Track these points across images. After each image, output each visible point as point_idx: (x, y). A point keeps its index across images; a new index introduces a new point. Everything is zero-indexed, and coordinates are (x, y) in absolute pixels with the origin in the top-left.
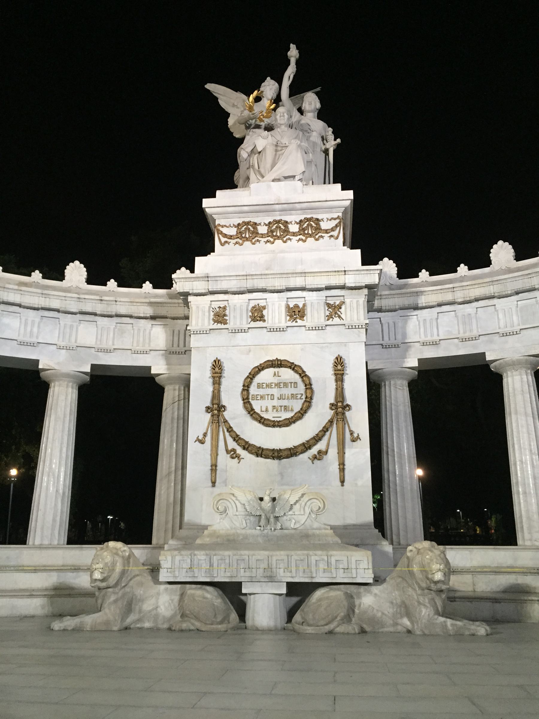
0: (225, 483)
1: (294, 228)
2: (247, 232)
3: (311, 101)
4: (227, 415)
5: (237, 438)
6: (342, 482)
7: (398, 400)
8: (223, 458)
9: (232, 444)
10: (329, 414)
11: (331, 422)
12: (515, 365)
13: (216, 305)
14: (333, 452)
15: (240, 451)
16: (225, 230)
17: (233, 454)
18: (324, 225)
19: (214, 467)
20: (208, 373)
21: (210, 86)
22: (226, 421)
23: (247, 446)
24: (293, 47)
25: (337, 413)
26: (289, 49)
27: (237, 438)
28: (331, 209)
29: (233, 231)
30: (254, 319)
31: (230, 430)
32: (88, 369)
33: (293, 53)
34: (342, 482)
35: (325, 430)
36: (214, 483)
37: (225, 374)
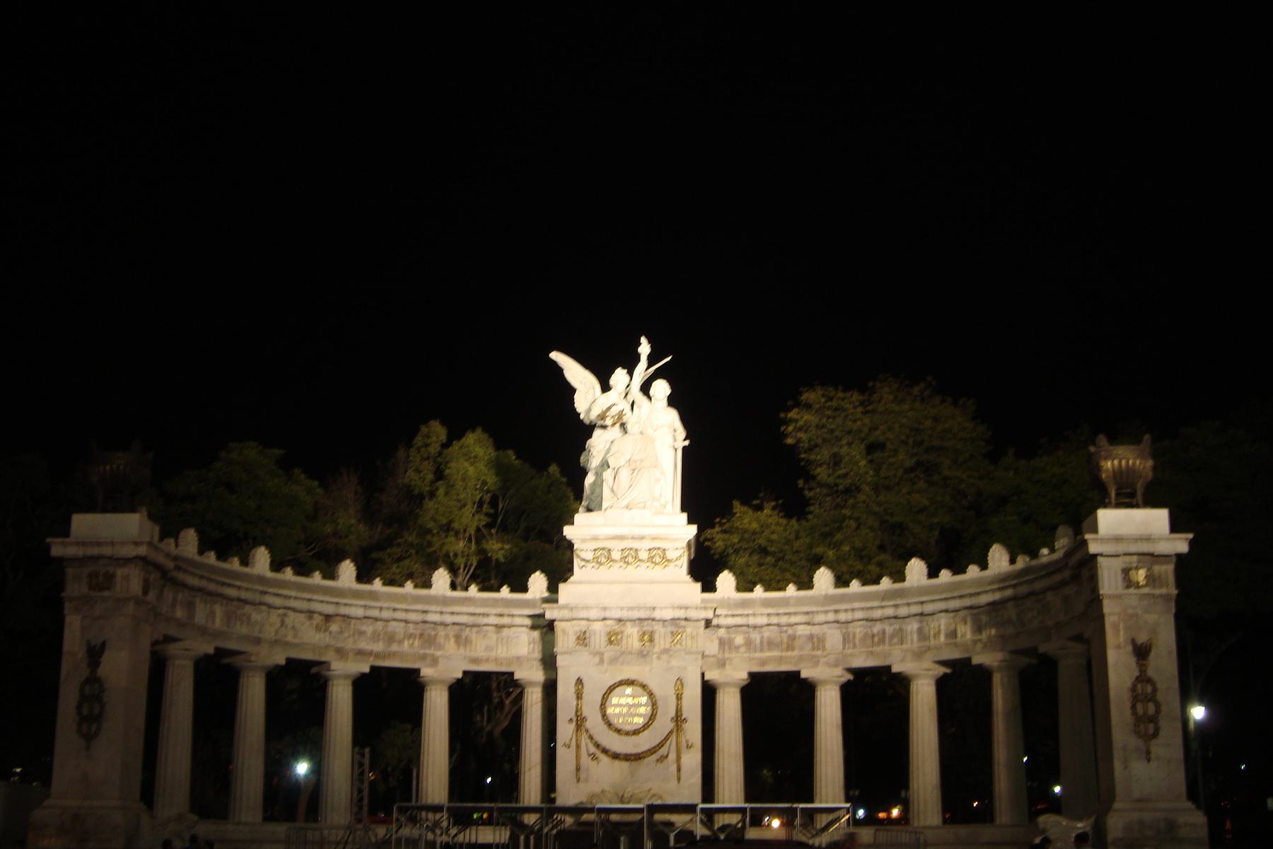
0: (586, 780)
1: (643, 555)
2: (604, 556)
3: (662, 388)
4: (588, 724)
5: (597, 745)
6: (679, 779)
7: (730, 708)
8: (585, 759)
9: (593, 749)
10: (671, 725)
11: (671, 732)
12: (825, 682)
13: (577, 628)
14: (672, 756)
15: (598, 753)
16: (583, 555)
17: (594, 757)
18: (670, 555)
19: (578, 769)
20: (572, 689)
21: (555, 356)
22: (587, 731)
23: (605, 751)
24: (643, 340)
25: (677, 726)
26: (640, 344)
27: (597, 745)
28: (675, 540)
29: (589, 556)
30: (611, 642)
31: (591, 738)
32: (460, 675)
33: (645, 348)
34: (679, 779)
35: (666, 739)
36: (578, 780)
37: (586, 691)
